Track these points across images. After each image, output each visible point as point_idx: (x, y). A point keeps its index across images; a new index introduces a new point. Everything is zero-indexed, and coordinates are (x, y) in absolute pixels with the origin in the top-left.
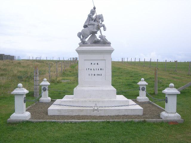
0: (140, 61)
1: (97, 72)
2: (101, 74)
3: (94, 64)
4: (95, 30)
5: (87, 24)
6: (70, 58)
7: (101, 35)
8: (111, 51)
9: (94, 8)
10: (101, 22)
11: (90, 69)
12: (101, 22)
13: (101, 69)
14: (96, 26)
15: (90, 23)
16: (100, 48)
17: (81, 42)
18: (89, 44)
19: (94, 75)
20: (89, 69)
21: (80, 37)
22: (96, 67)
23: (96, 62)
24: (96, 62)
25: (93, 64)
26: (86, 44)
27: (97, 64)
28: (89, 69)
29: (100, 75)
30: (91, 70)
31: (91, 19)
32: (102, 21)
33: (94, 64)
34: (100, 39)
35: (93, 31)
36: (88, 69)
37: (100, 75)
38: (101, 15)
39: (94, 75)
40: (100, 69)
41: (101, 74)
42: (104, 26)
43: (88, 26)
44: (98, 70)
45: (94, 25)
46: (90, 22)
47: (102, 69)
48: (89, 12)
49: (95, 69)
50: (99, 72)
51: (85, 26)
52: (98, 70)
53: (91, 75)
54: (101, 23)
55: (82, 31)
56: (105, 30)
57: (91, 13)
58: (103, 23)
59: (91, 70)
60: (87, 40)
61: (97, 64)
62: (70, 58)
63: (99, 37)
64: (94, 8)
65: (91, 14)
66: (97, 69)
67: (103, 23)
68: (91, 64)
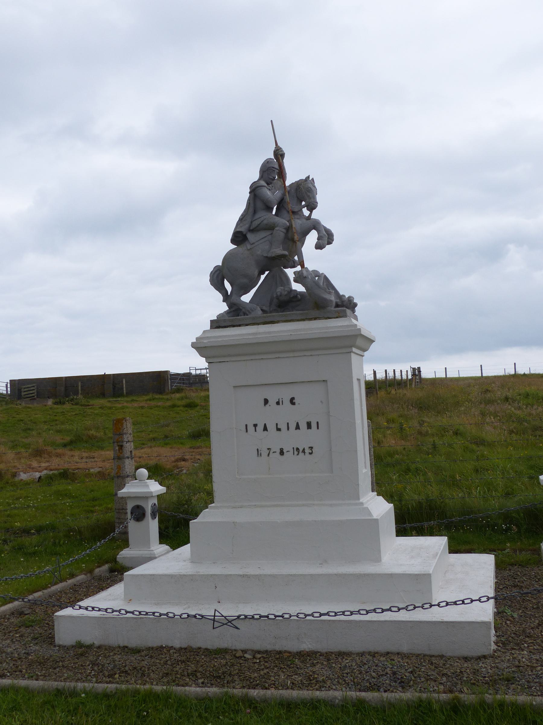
0: (448, 376)
2: (311, 448)
3: (278, 403)
4: (279, 251)
5: (243, 229)
10: (306, 212)
11: (260, 428)
12: (306, 212)
13: (309, 425)
14: (280, 233)
17: (224, 308)
19: (282, 453)
20: (255, 426)
21: (220, 287)
23: (286, 394)
24: (286, 394)
26: (245, 314)
27: (292, 401)
28: (255, 426)
29: (307, 451)
30: (265, 429)
31: (259, 204)
32: (312, 207)
33: (278, 403)
34: (298, 287)
35: (269, 255)
36: (251, 428)
37: (307, 451)
39: (282, 453)
40: (303, 426)
41: (311, 448)
43: (250, 236)
44: (298, 427)
45: (271, 228)
46: (257, 216)
47: (314, 425)
49: (283, 427)
52: (298, 427)
53: (265, 453)
54: (309, 217)
55: (228, 258)
57: (262, 177)
58: (316, 215)
59: (265, 429)
60: (246, 298)
61: (292, 401)
63: (295, 281)
64: (279, 154)
65: (263, 183)
66: (293, 426)
67: (316, 215)
68: (266, 402)
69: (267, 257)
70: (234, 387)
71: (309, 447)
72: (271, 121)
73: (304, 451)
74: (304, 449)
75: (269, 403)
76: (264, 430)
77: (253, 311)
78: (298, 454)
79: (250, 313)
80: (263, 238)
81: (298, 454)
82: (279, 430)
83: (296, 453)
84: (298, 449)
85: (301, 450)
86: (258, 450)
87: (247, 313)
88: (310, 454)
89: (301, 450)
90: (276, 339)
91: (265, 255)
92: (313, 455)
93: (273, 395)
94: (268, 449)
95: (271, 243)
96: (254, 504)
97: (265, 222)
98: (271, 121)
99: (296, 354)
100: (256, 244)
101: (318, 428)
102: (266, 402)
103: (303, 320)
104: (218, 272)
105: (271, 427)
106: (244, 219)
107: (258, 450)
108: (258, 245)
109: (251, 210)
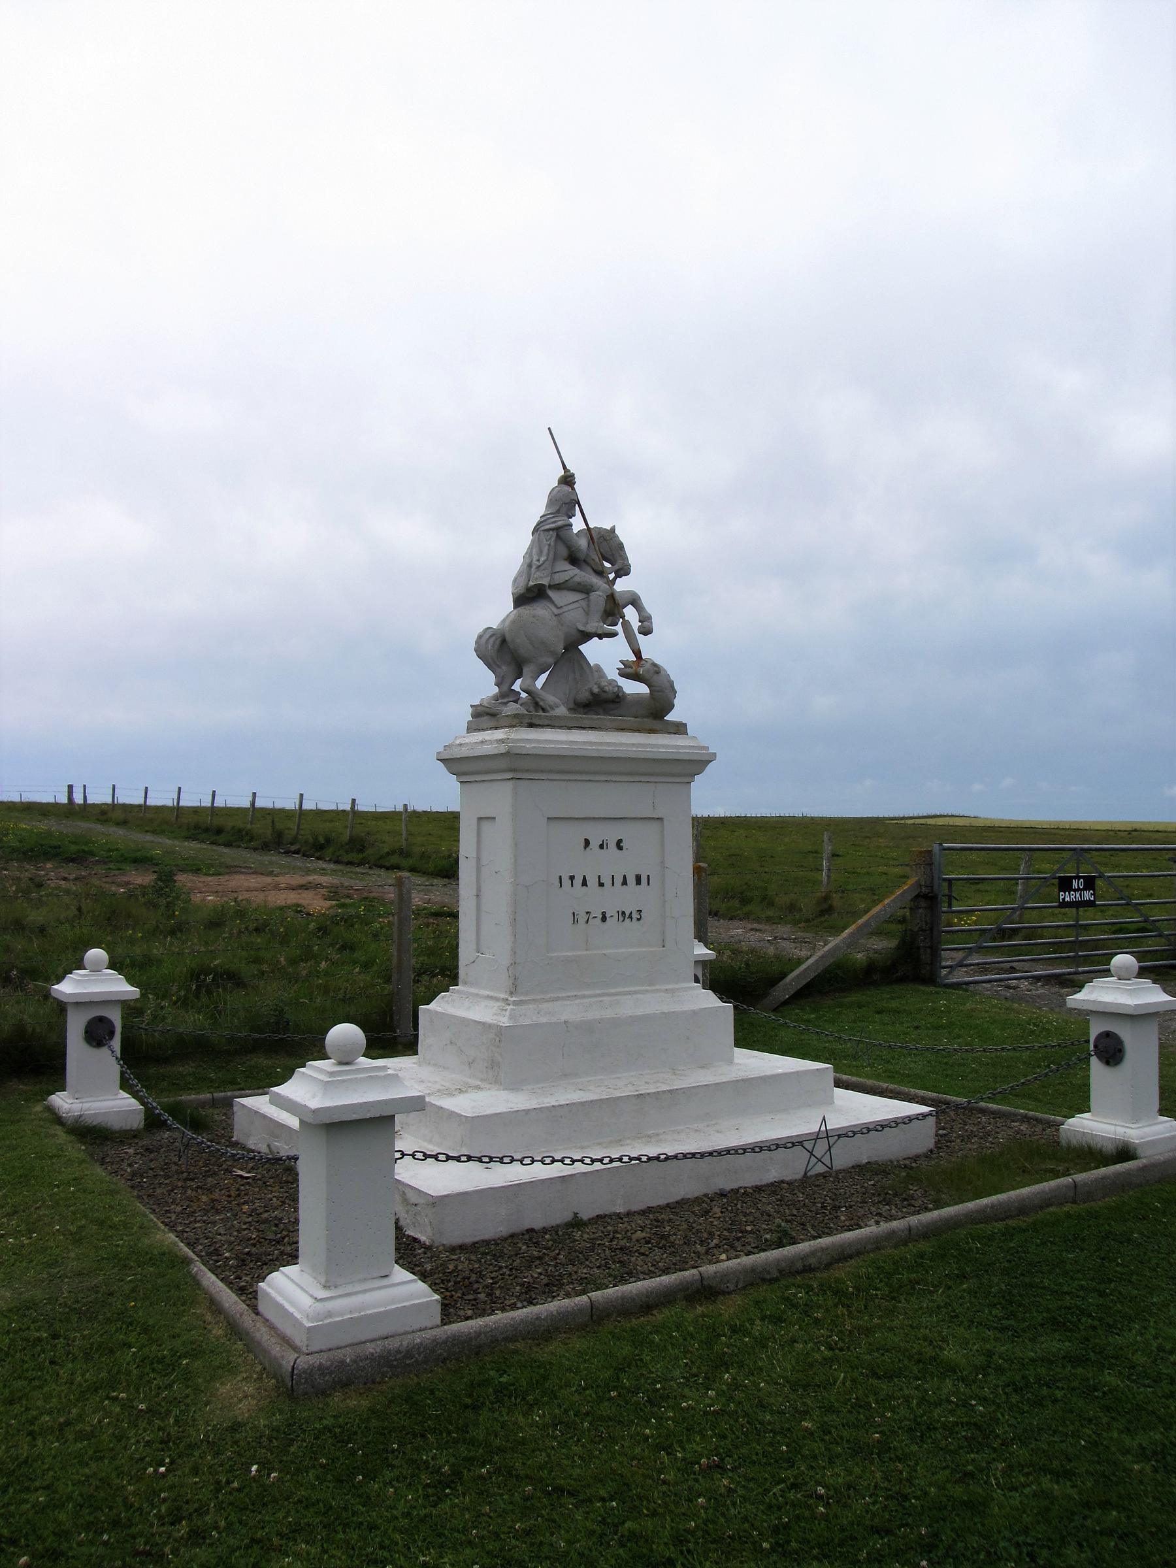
1: (615, 899)
3: (601, 847)
5: (545, 582)
6: (70, 787)
7: (638, 654)
8: (696, 764)
9: (568, 480)
11: (578, 881)
13: (638, 880)
14: (598, 599)
15: (560, 578)
16: (639, 745)
18: (562, 711)
19: (604, 919)
20: (572, 878)
22: (610, 864)
23: (611, 833)
24: (611, 833)
25: (594, 844)
28: (572, 878)
29: (635, 916)
30: (584, 883)
31: (563, 551)
32: (623, 571)
36: (566, 882)
38: (613, 530)
39: (604, 919)
40: (631, 880)
42: (635, 601)
43: (550, 593)
44: (625, 883)
47: (644, 880)
48: (537, 508)
49: (607, 880)
50: (629, 897)
51: (528, 596)
52: (625, 883)
53: (582, 918)
55: (516, 624)
56: (646, 631)
59: (584, 883)
61: (619, 845)
62: (70, 787)
64: (568, 480)
67: (622, 585)
68: (587, 843)
69: (582, 632)
70: (548, 818)
71: (638, 911)
72: (549, 429)
73: (630, 917)
74: (631, 913)
75: (591, 846)
76: (583, 885)
77: (557, 707)
78: (623, 921)
79: (553, 709)
80: (573, 602)
81: (623, 921)
82: (601, 885)
83: (621, 918)
84: (623, 913)
85: (627, 915)
86: (574, 913)
87: (549, 709)
88: (639, 919)
89: (627, 915)
90: (620, 755)
91: (582, 628)
92: (641, 921)
93: (596, 834)
94: (587, 913)
95: (587, 614)
96: (572, 994)
97: (577, 579)
98: (549, 429)
99: (597, 778)
100: (565, 609)
101: (648, 884)
102: (587, 843)
103: (639, 731)
104: (494, 638)
105: (592, 881)
106: (542, 567)
107: (574, 913)
108: (569, 611)
109: (551, 556)
